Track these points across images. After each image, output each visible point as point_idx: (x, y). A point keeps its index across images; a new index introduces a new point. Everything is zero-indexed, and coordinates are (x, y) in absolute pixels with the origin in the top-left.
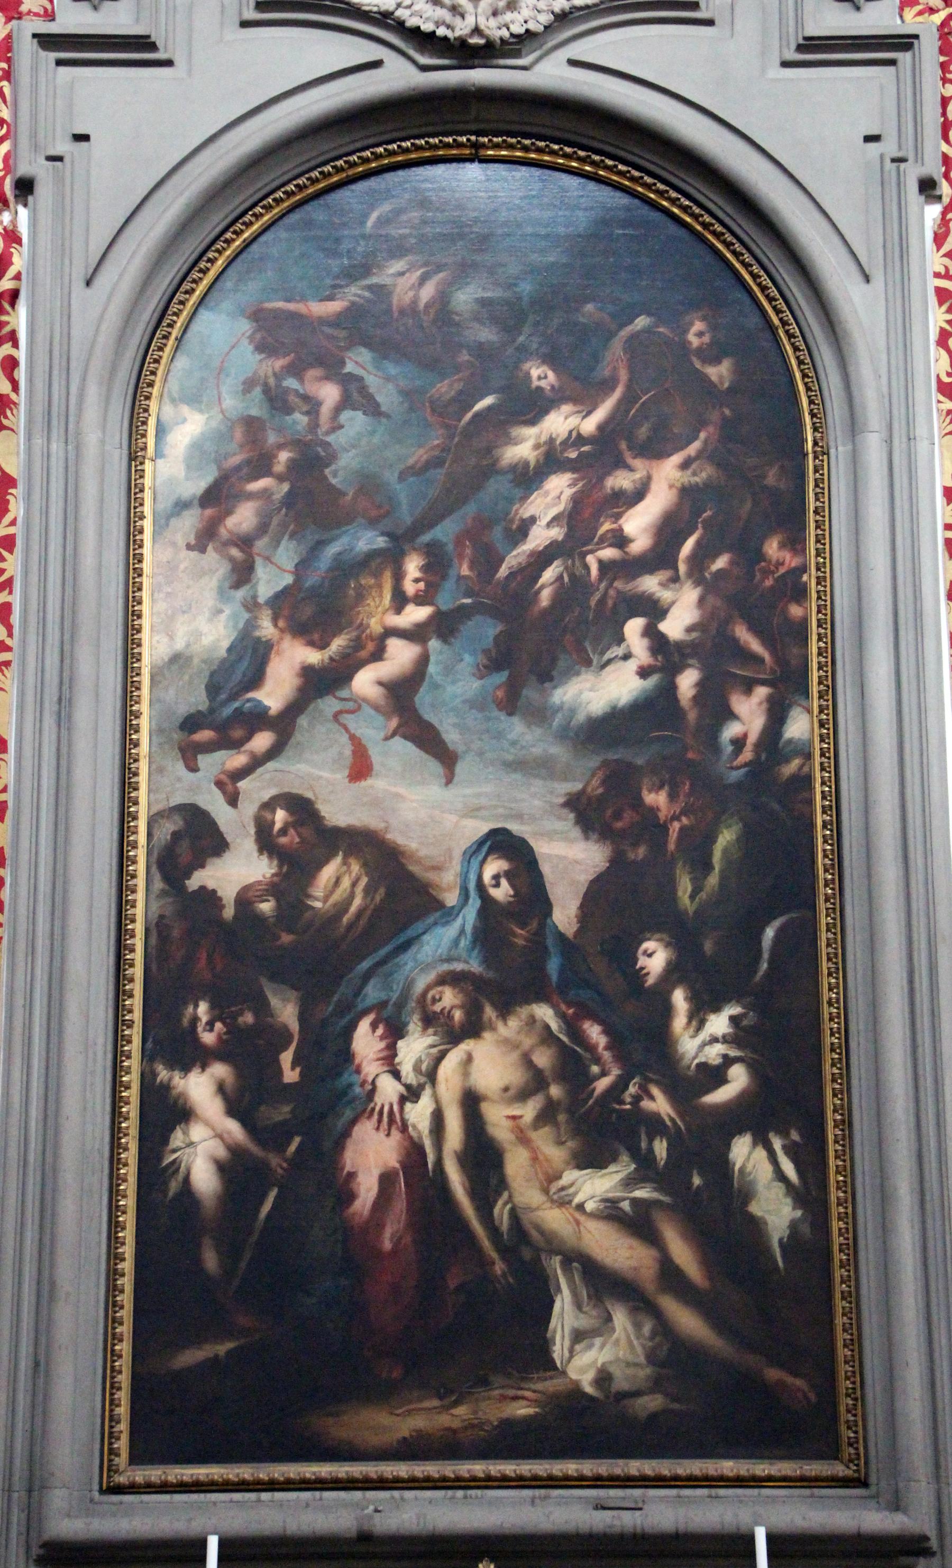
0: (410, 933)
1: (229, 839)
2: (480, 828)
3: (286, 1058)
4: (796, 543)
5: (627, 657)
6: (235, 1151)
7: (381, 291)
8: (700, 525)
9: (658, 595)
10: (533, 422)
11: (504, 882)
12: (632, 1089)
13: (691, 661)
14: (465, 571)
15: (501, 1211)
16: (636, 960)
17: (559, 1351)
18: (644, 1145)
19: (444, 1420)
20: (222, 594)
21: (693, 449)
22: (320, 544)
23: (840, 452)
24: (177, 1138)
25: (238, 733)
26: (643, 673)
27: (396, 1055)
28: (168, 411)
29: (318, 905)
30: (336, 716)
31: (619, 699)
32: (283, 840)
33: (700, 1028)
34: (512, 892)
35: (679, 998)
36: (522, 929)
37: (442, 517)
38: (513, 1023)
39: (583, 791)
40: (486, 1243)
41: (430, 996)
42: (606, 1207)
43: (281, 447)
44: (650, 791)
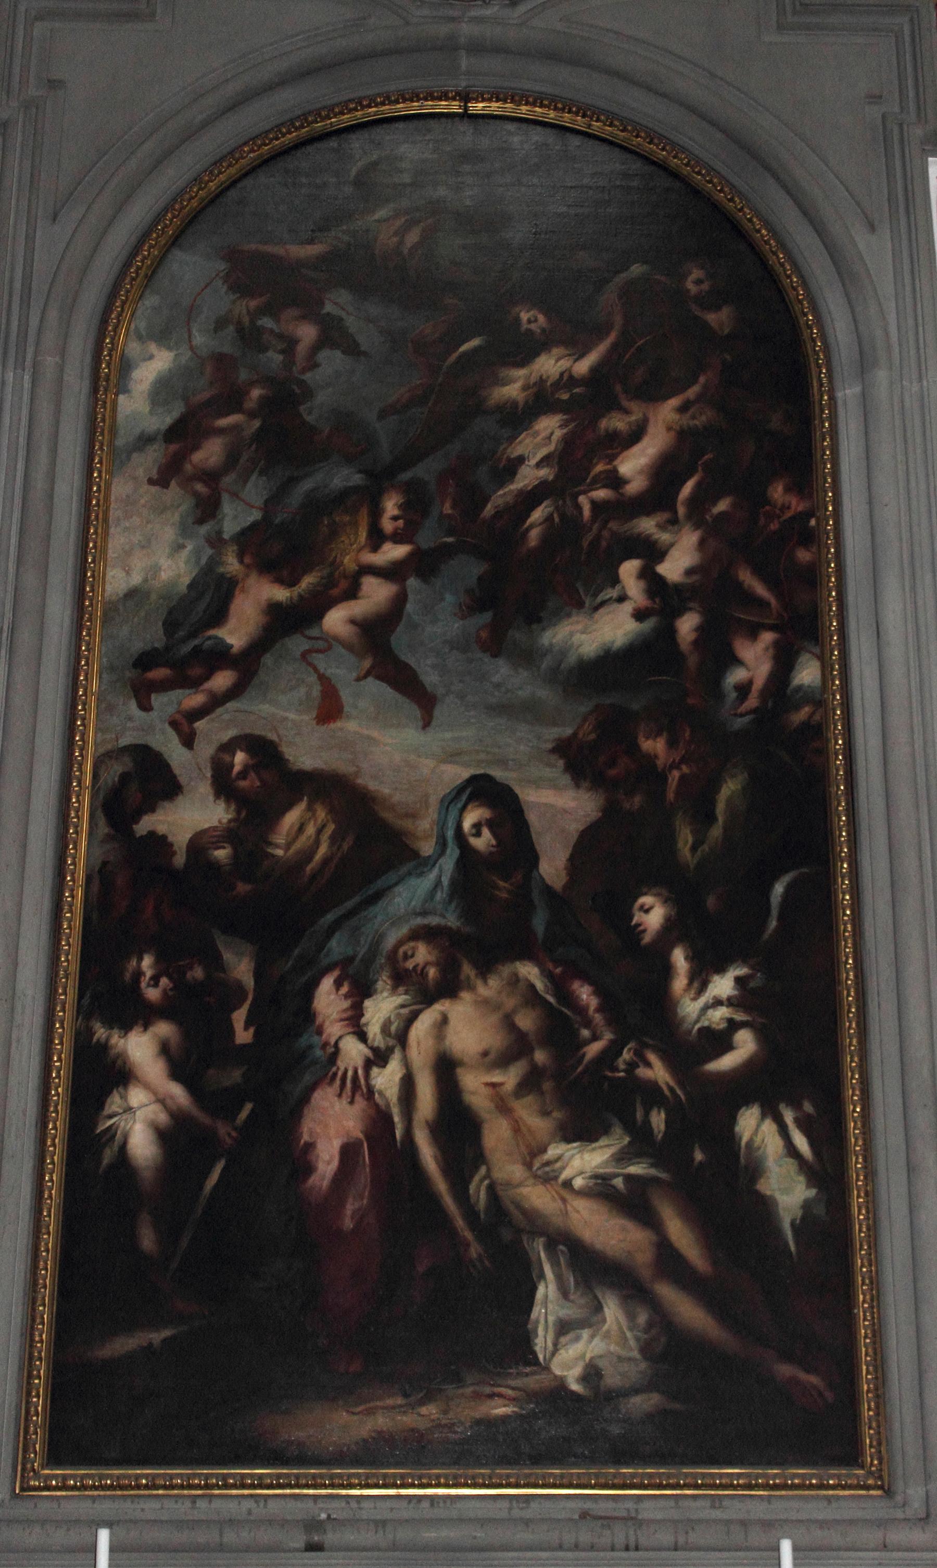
0: (380, 884)
1: (183, 780)
3: (239, 1017)
5: (622, 599)
6: (179, 1118)
8: (700, 468)
11: (486, 832)
12: (626, 1055)
13: (692, 605)
14: (447, 509)
16: (631, 917)
17: (542, 1342)
18: (639, 1115)
19: (408, 1420)
20: (184, 531)
21: (692, 392)
22: (292, 481)
24: (114, 1103)
25: (196, 671)
26: (639, 615)
29: (280, 852)
30: (304, 655)
31: (613, 642)
32: (243, 784)
34: (494, 842)
35: (679, 958)
38: (494, 982)
40: (460, 1222)
42: (596, 1184)
43: (252, 384)
44: (647, 738)
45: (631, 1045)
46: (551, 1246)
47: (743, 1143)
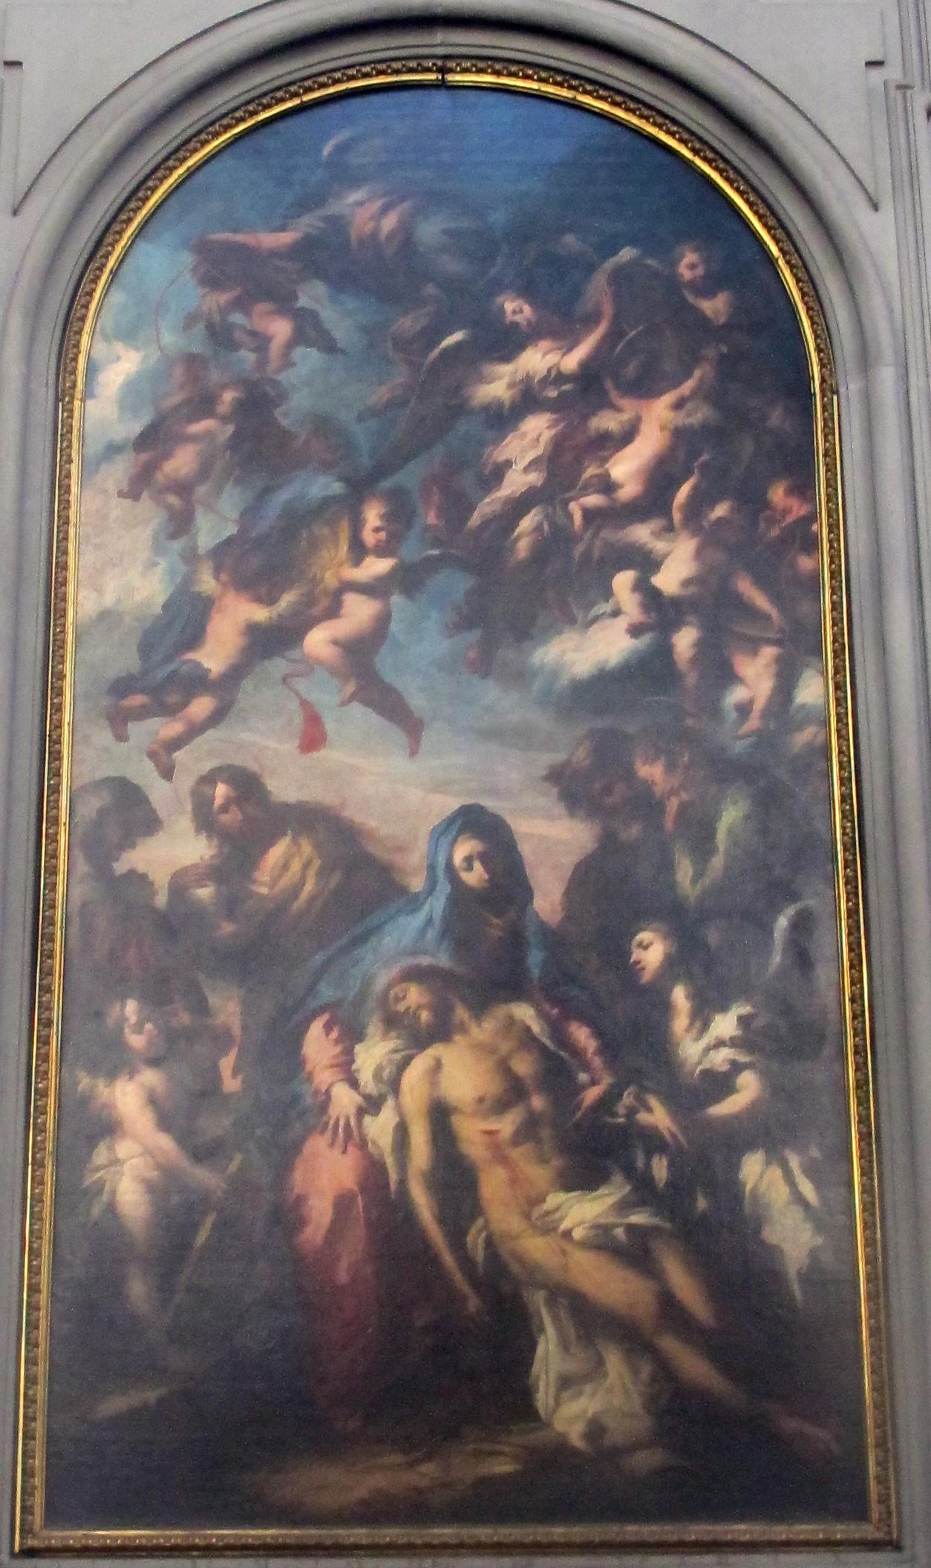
0: (372, 921)
1: (162, 814)
2: (452, 804)
3: (227, 1064)
4: (804, 488)
5: (616, 613)
6: (168, 1171)
7: (338, 225)
8: (696, 471)
9: (650, 546)
10: (507, 358)
11: (477, 865)
12: (628, 1099)
13: (690, 618)
14: (431, 518)
15: (475, 1240)
16: (630, 954)
17: (543, 1398)
18: (640, 1163)
20: (158, 548)
22: (267, 491)
23: (851, 387)
24: (101, 1155)
25: (172, 699)
26: (635, 631)
27: (353, 1061)
28: (100, 349)
29: (264, 890)
31: (607, 661)
32: (225, 818)
33: (706, 1026)
34: (486, 877)
35: (680, 996)
36: (498, 916)
37: (407, 459)
39: (567, 763)
40: (458, 1278)
41: (392, 993)
42: (596, 1235)
43: (224, 387)
44: (644, 764)
45: (631, 1089)
46: (552, 1301)
47: (748, 1188)
